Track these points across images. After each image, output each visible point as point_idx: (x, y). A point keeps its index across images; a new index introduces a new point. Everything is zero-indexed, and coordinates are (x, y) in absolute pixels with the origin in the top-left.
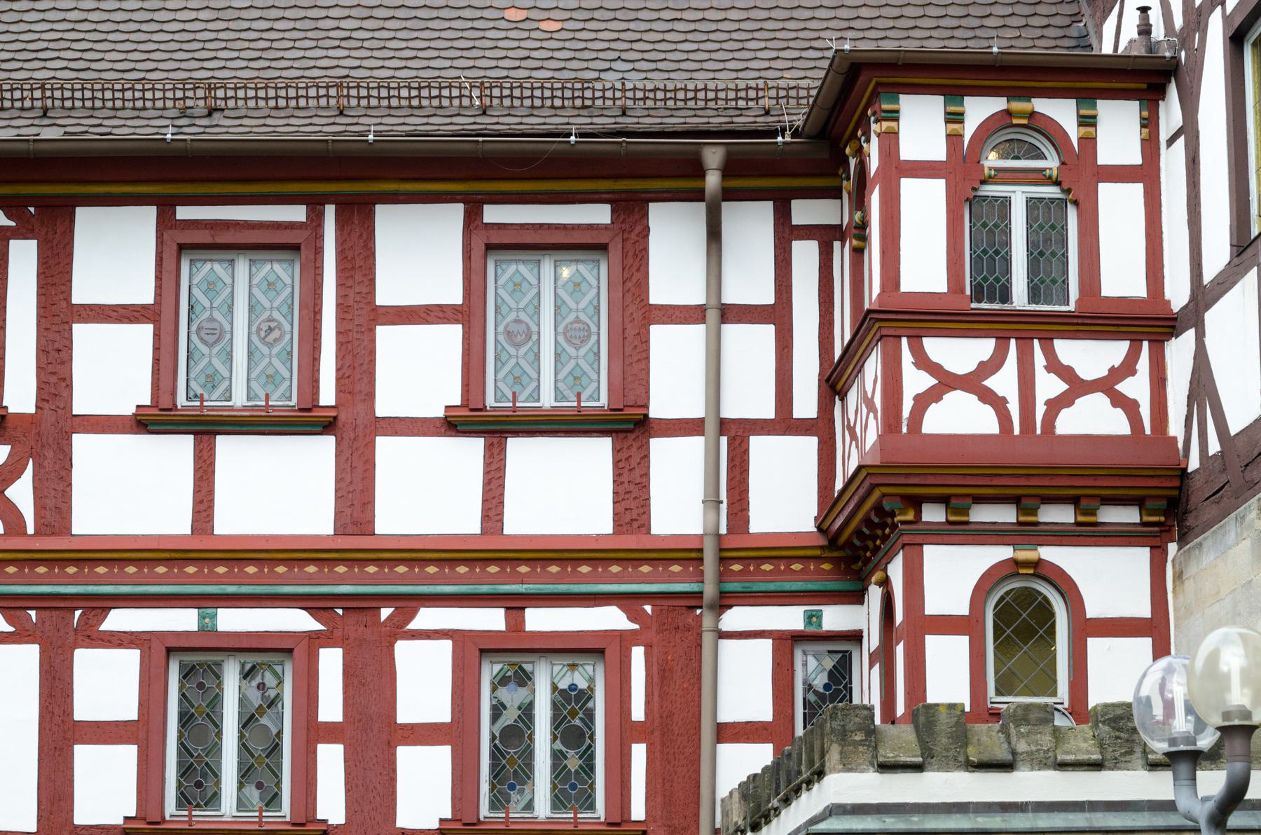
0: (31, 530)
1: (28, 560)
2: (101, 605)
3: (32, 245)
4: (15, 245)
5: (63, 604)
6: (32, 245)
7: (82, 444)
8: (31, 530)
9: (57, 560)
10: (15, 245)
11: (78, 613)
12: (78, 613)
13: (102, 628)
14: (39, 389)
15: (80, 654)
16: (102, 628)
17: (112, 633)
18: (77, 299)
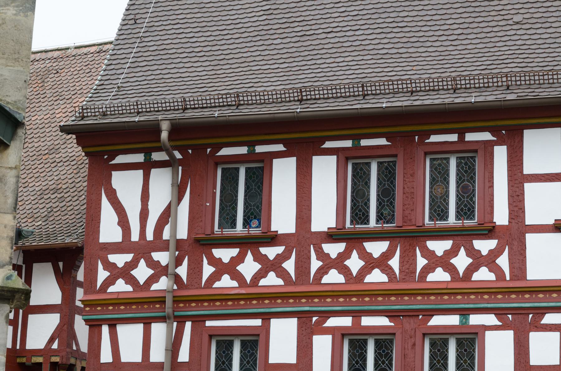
0: (508, 278)
1: (507, 292)
2: (542, 312)
3: (504, 148)
4: (496, 148)
5: (524, 311)
6: (504, 148)
7: (529, 237)
8: (508, 278)
9: (520, 292)
10: (496, 148)
11: (531, 316)
12: (531, 316)
13: (542, 322)
14: (510, 214)
15: (533, 336)
16: (542, 322)
17: (547, 325)
18: (526, 172)
